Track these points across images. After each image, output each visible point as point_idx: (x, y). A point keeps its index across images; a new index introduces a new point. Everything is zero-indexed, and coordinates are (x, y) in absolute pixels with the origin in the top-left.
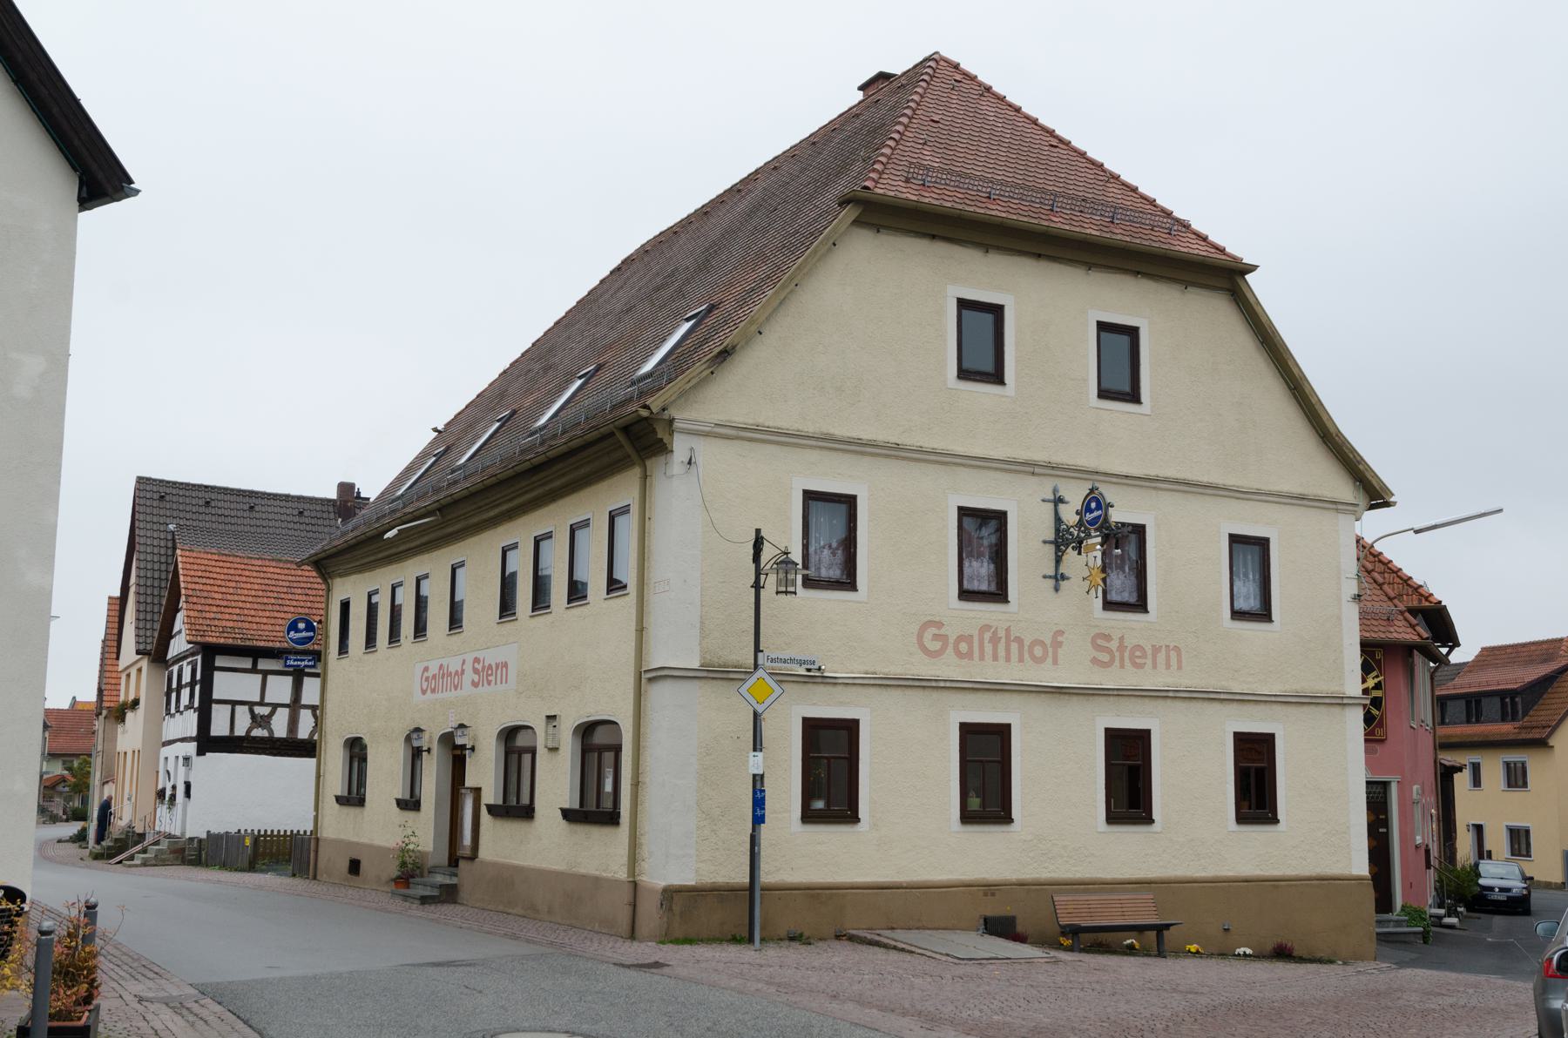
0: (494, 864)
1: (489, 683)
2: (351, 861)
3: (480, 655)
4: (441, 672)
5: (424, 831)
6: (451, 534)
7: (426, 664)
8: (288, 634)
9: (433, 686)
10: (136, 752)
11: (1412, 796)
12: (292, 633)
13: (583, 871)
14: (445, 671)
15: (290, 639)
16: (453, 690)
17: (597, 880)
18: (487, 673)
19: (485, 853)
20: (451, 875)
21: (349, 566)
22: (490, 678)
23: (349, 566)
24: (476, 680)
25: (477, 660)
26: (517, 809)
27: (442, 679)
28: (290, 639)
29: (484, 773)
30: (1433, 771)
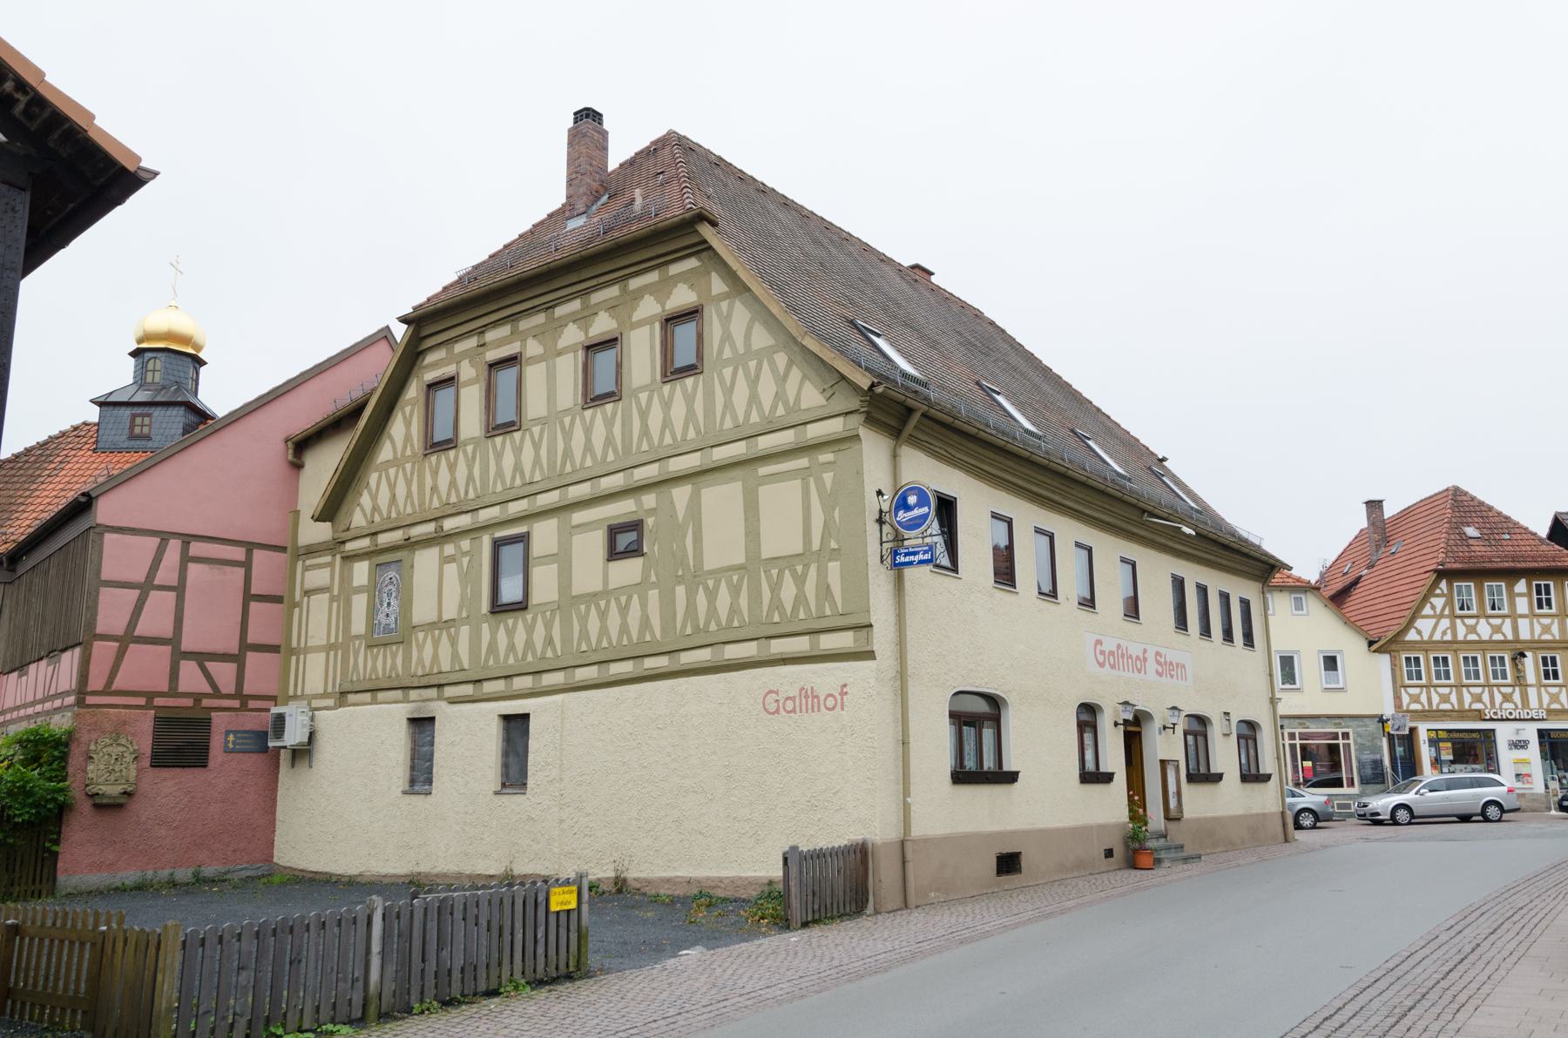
0: (1198, 820)
1: (1172, 676)
2: (998, 857)
3: (1163, 651)
4: (1120, 652)
5: (1110, 804)
6: (1134, 534)
7: (1100, 637)
8: (896, 516)
9: (1112, 663)
10: (816, 709)
11: (291, 644)
12: (901, 513)
13: (1254, 812)
14: (1125, 652)
15: (897, 522)
16: (1136, 671)
17: (1264, 815)
18: (1168, 668)
19: (1187, 814)
20: (1157, 838)
21: (965, 458)
22: (1172, 673)
23: (965, 458)
24: (1161, 671)
25: (1158, 654)
26: (1203, 776)
27: (1113, 658)
28: (897, 522)
29: (1164, 746)
30: (239, 619)
